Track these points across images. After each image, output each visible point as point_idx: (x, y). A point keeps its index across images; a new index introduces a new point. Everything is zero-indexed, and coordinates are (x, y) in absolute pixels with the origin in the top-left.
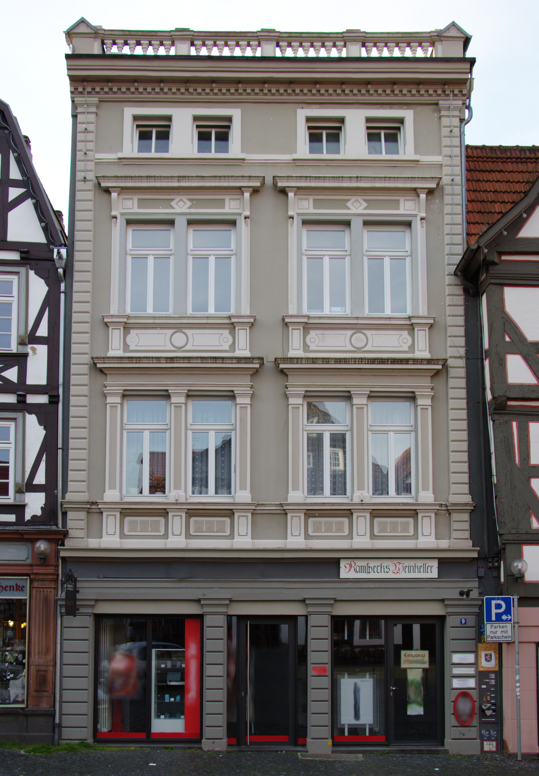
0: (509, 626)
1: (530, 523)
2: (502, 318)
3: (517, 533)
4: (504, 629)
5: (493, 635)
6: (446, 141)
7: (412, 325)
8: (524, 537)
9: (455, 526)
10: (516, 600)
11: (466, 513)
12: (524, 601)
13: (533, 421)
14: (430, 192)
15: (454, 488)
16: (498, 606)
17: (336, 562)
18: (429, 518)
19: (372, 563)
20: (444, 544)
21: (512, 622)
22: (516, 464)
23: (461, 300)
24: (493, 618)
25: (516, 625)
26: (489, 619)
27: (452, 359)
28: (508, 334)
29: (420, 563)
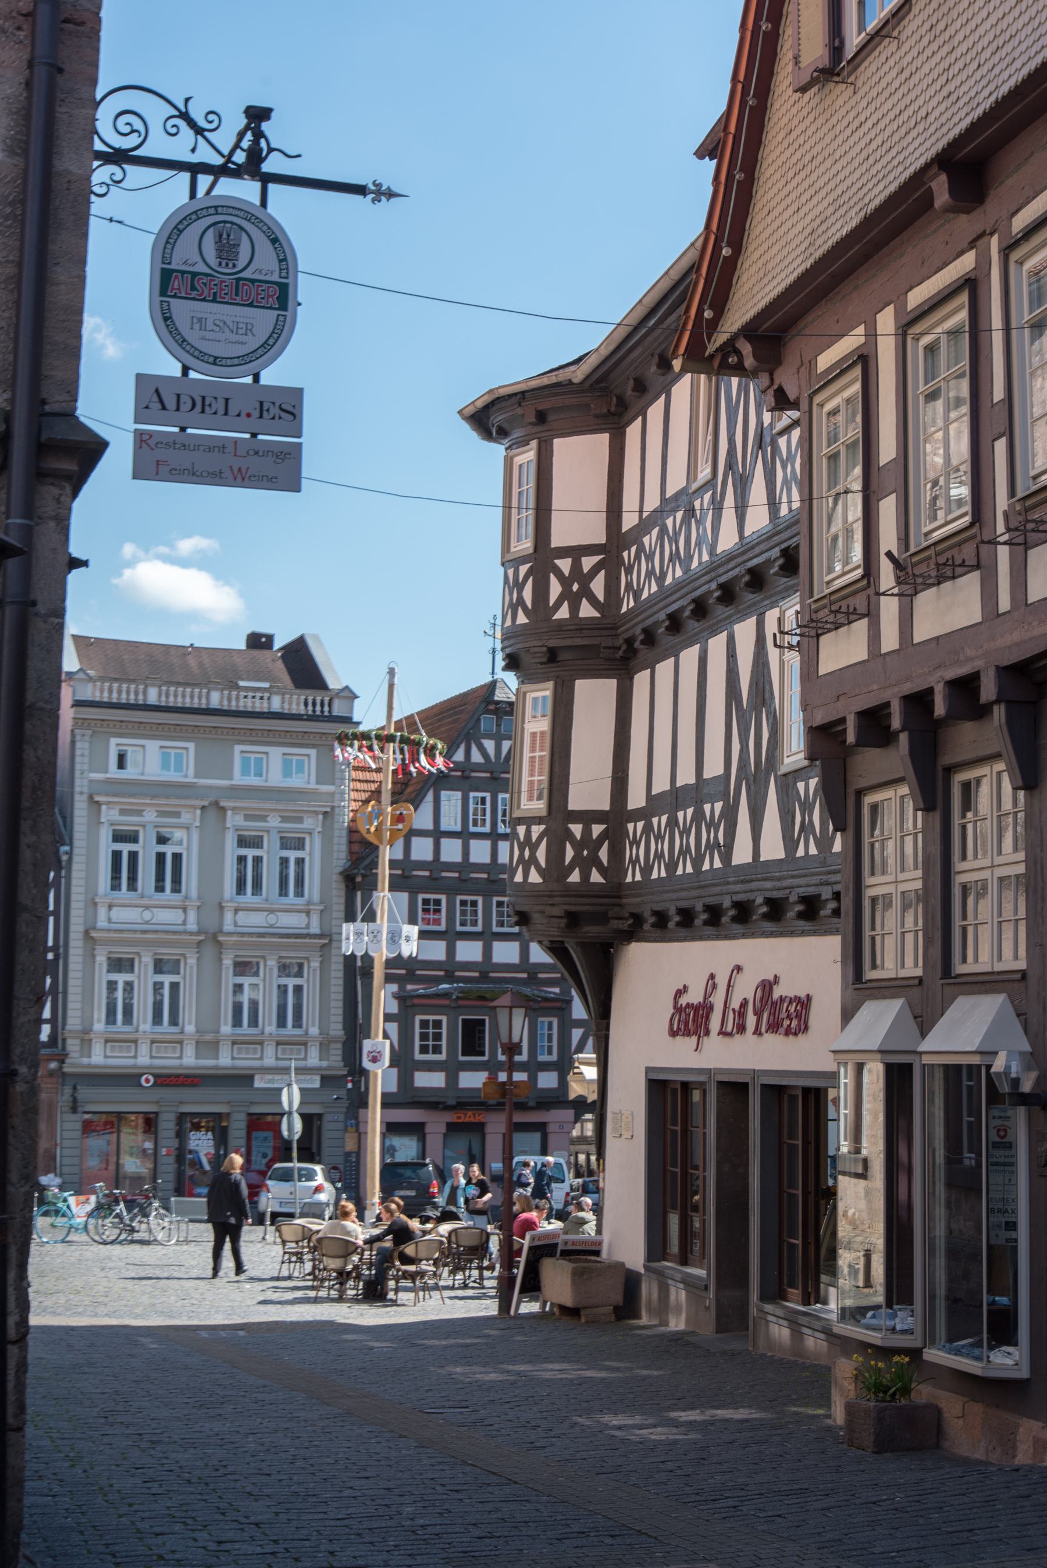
14: (325, 813)
17: (251, 1078)
19: (277, 1077)
20: (325, 1064)
23: (343, 893)
29: (308, 1077)
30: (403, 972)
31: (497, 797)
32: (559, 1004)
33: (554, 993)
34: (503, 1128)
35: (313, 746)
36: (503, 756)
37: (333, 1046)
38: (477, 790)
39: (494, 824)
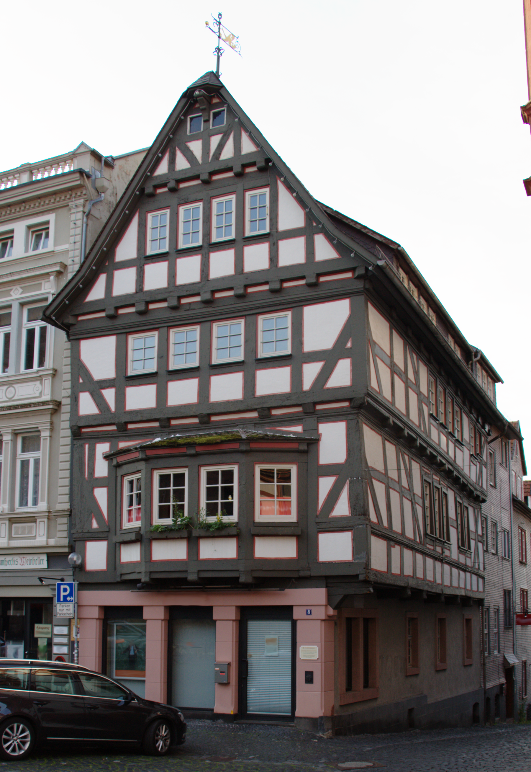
0: (71, 605)
1: (91, 524)
2: (78, 365)
3: (82, 532)
4: (68, 608)
5: (60, 612)
6: (72, 232)
7: (40, 376)
8: (87, 535)
9: (60, 528)
10: (76, 585)
11: (66, 517)
12: (83, 586)
13: (99, 442)
16: (65, 590)
18: (43, 522)
20: (52, 542)
21: (74, 602)
22: (85, 478)
24: (62, 599)
25: (76, 605)
26: (59, 600)
27: (64, 399)
28: (81, 377)
32: (294, 446)
33: (294, 433)
34: (232, 614)
39: (207, 234)
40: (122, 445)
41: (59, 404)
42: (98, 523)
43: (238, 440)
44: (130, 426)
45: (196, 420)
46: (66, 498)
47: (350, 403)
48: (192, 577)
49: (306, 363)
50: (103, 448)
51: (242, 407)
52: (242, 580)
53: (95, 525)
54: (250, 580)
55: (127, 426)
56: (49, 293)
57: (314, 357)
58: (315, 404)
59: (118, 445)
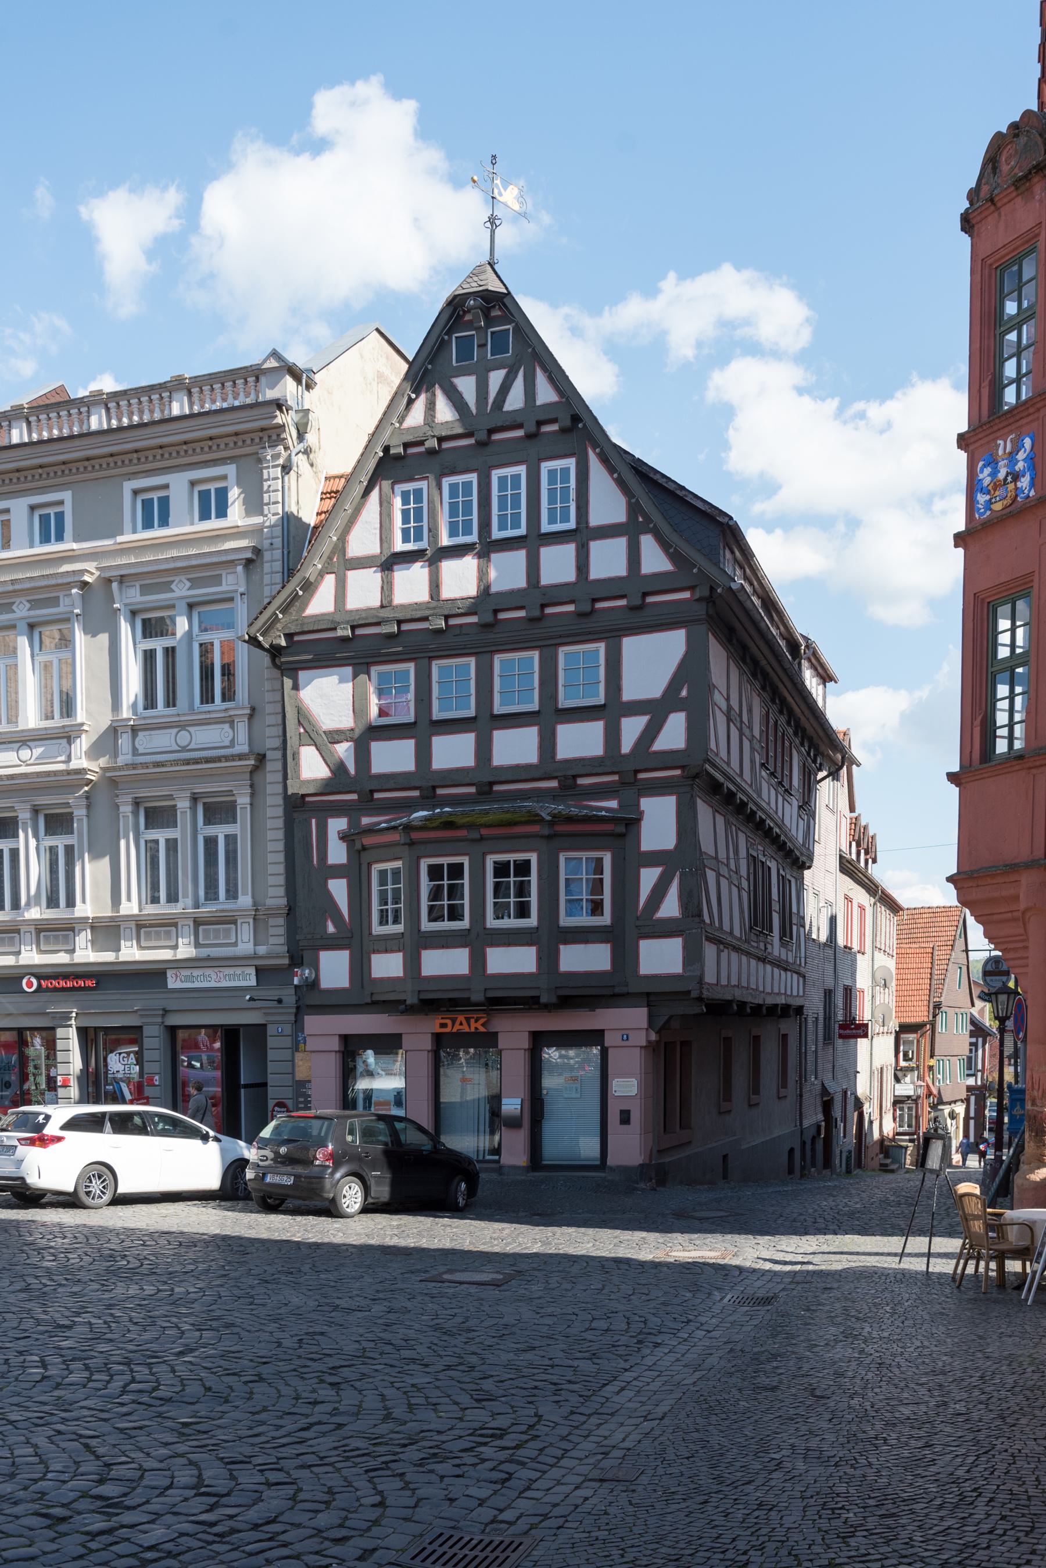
1: (325, 927)
9: (272, 931)
13: (332, 817)
14: (249, 562)
15: (272, 892)
20: (262, 950)
29: (239, 971)
30: (354, 797)
31: (488, 477)
33: (608, 810)
35: (231, 459)
36: (491, 400)
37: (272, 921)
38: (453, 472)
40: (365, 821)
41: (261, 758)
42: (335, 927)
43: (534, 819)
44: (377, 795)
45: (472, 790)
46: (281, 891)
47: (683, 772)
48: (477, 997)
49: (625, 716)
50: (337, 825)
51: (536, 775)
52: (544, 1000)
53: (331, 929)
54: (554, 1000)
55: (372, 795)
56: (236, 591)
57: (636, 708)
58: (637, 772)
59: (360, 821)
